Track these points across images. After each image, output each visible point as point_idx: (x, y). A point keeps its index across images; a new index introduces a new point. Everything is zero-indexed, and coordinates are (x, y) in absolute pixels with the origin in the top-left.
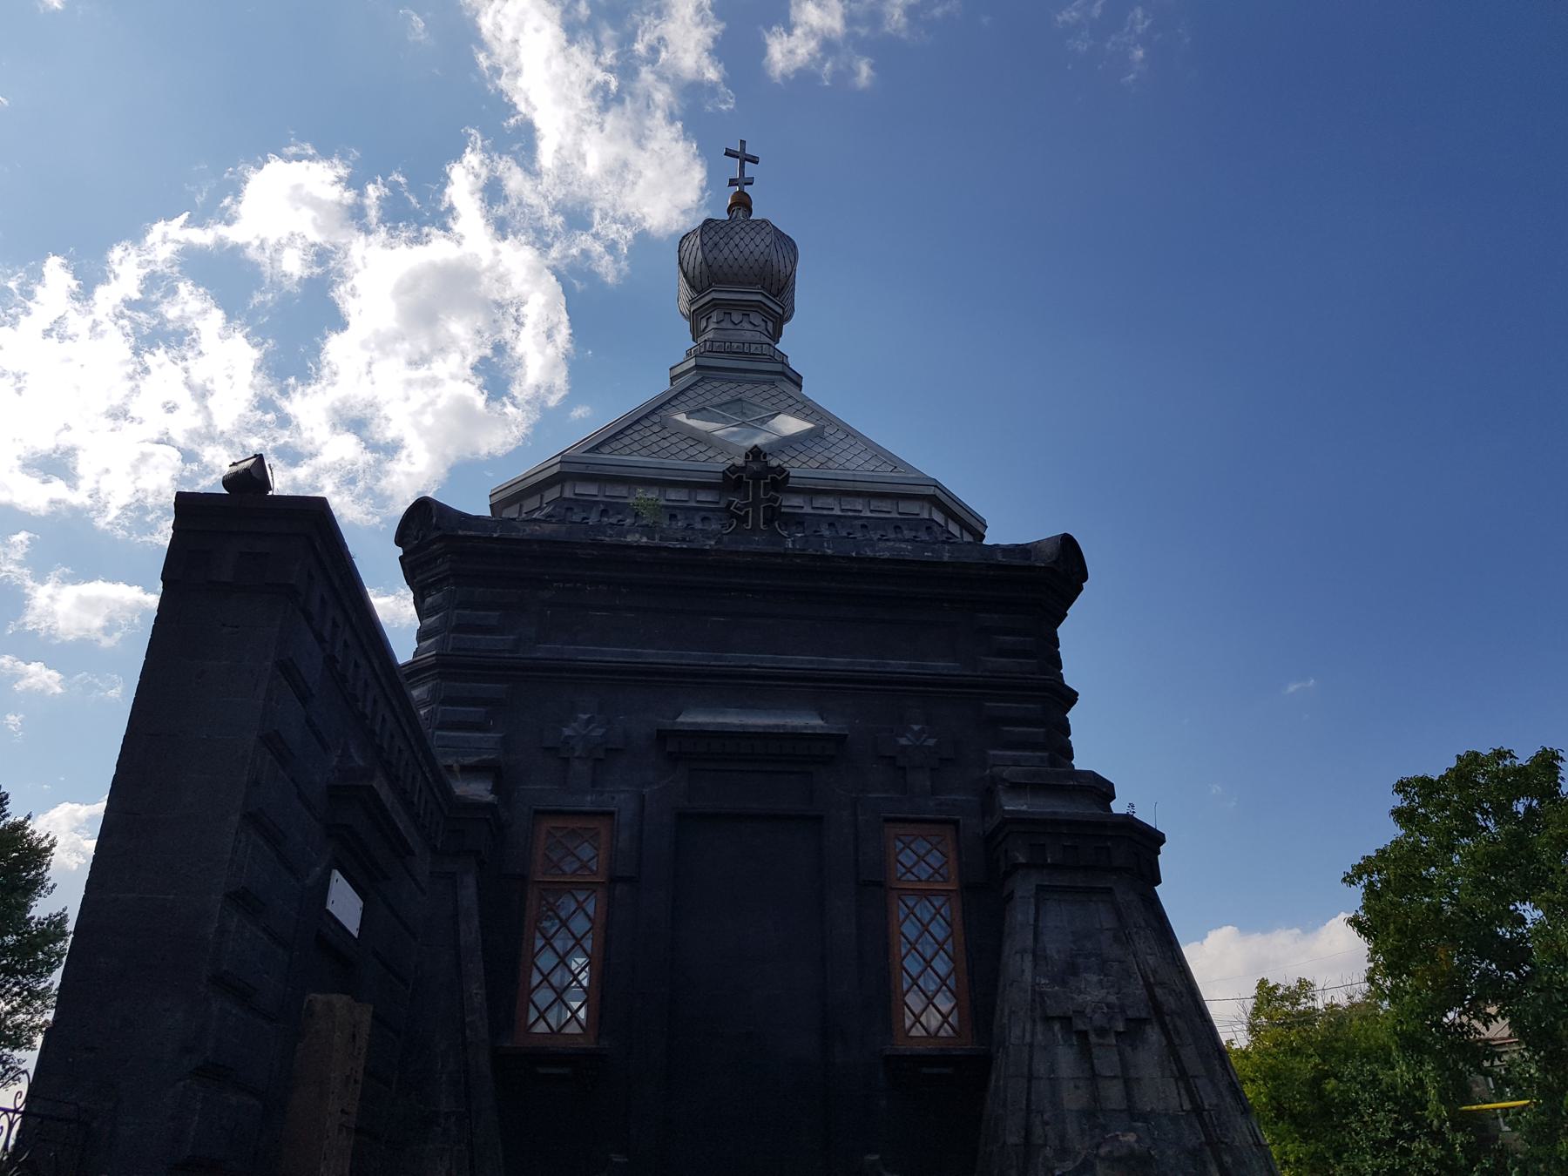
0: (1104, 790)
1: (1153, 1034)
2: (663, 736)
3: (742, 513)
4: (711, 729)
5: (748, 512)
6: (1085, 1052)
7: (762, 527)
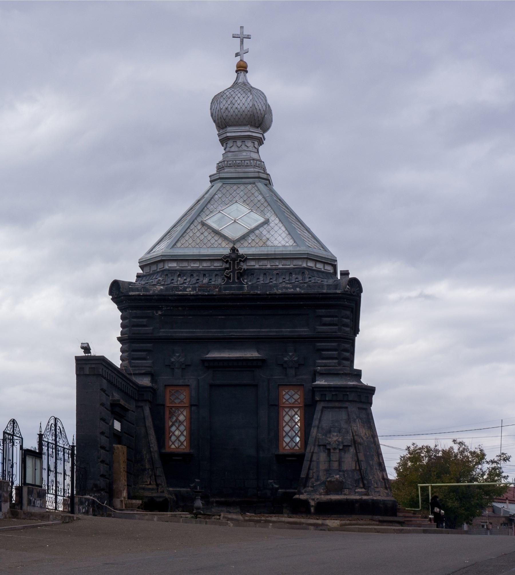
0: (356, 373)
1: (352, 450)
2: (204, 361)
3: (229, 276)
4: (218, 359)
5: (231, 275)
6: (329, 455)
7: (236, 281)
